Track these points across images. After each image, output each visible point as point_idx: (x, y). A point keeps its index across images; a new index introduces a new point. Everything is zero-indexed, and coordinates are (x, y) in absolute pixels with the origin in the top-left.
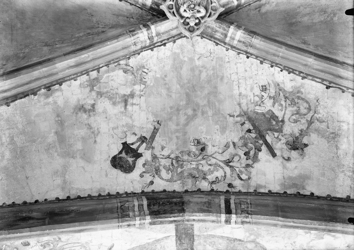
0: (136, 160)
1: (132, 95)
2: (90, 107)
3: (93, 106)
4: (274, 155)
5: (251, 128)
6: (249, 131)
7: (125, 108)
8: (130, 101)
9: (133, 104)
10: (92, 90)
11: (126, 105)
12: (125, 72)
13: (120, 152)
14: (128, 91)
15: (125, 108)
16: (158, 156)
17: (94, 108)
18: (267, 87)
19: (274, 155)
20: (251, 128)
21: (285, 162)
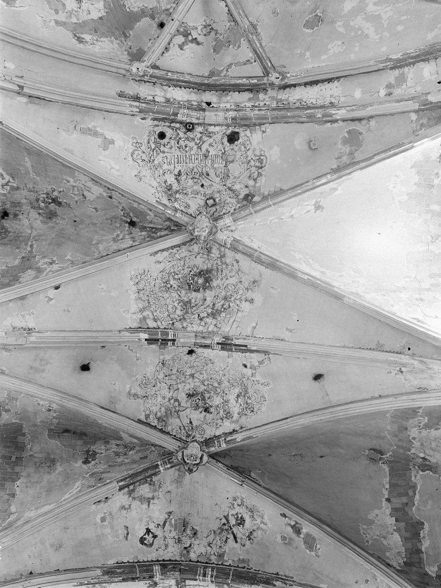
0: (154, 540)
1: (153, 498)
2: (128, 507)
3: (130, 506)
4: (236, 542)
5: (226, 523)
6: (224, 524)
7: (149, 507)
8: (152, 501)
9: (153, 503)
10: (130, 496)
11: (149, 505)
12: (150, 484)
13: (145, 535)
14: (150, 495)
15: (149, 507)
16: (167, 537)
17: (130, 507)
18: (237, 498)
19: (236, 542)
20: (226, 523)
21: (242, 547)
